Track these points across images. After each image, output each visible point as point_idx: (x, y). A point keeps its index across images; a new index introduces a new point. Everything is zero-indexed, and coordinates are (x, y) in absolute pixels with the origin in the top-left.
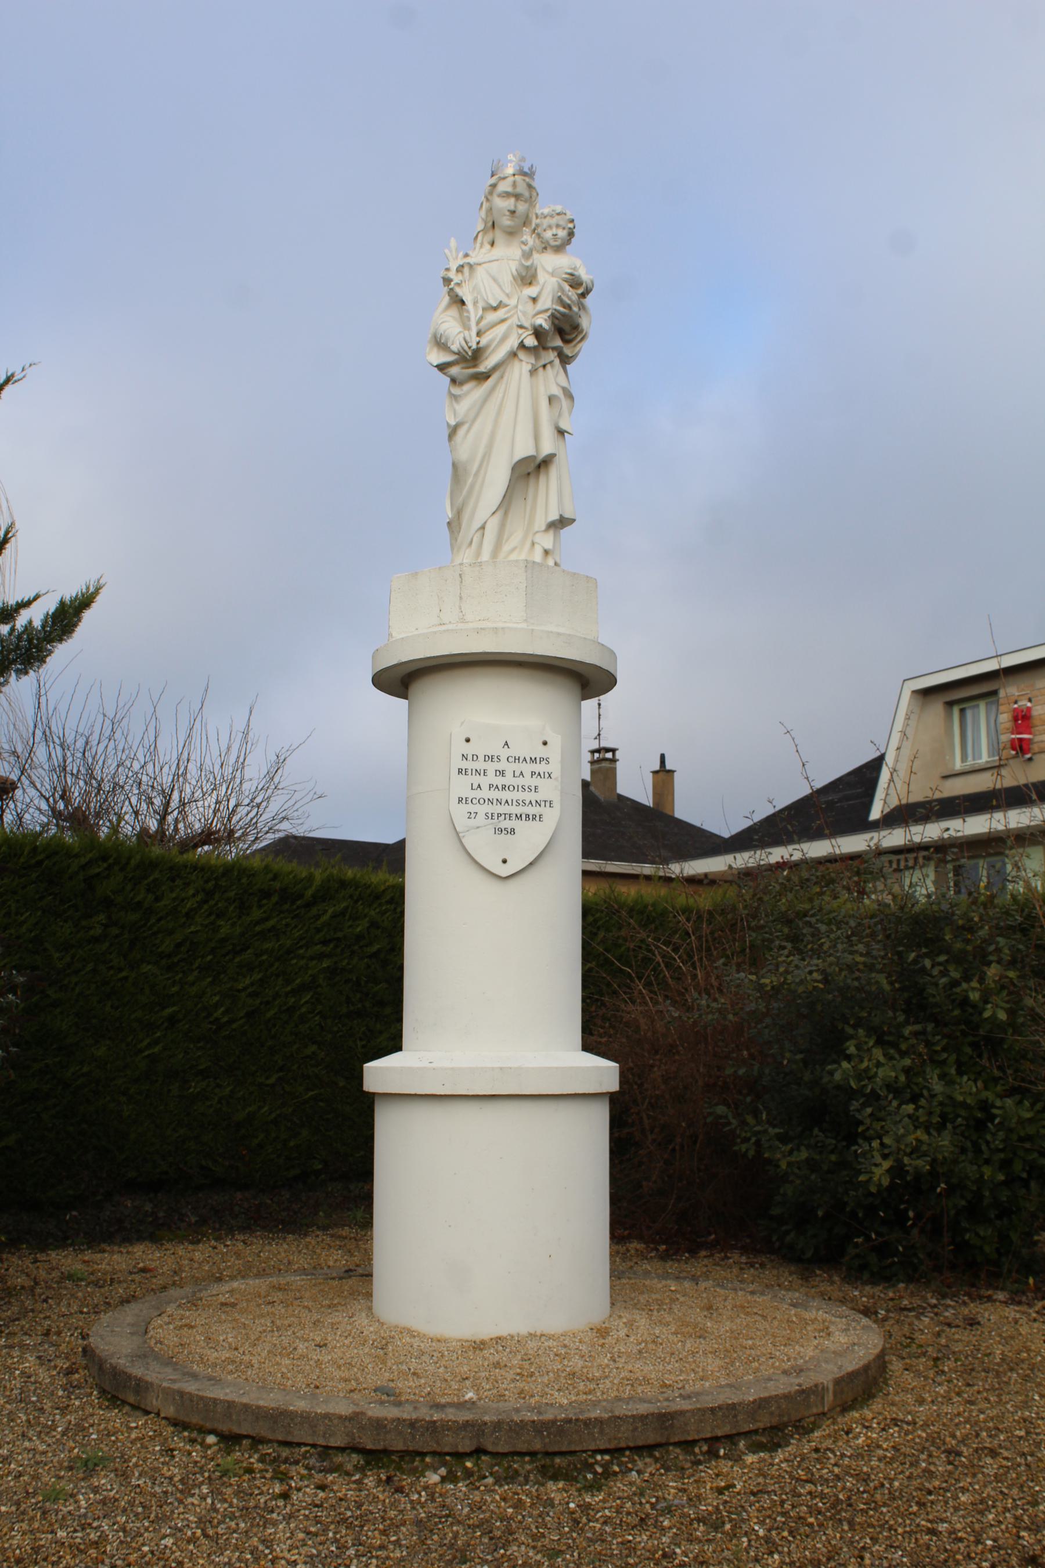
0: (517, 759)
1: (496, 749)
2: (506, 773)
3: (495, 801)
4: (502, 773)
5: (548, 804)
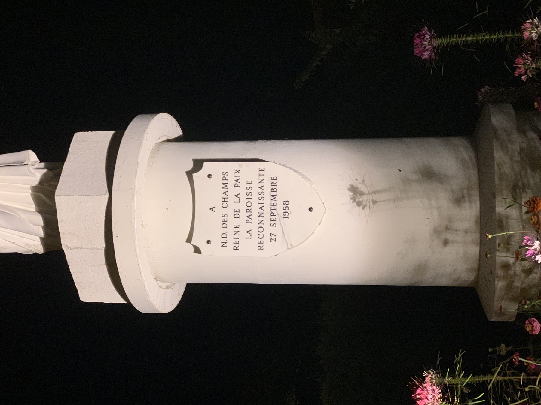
0: (225, 200)
1: (217, 218)
2: (237, 209)
3: (261, 218)
4: (237, 212)
5: (262, 173)
